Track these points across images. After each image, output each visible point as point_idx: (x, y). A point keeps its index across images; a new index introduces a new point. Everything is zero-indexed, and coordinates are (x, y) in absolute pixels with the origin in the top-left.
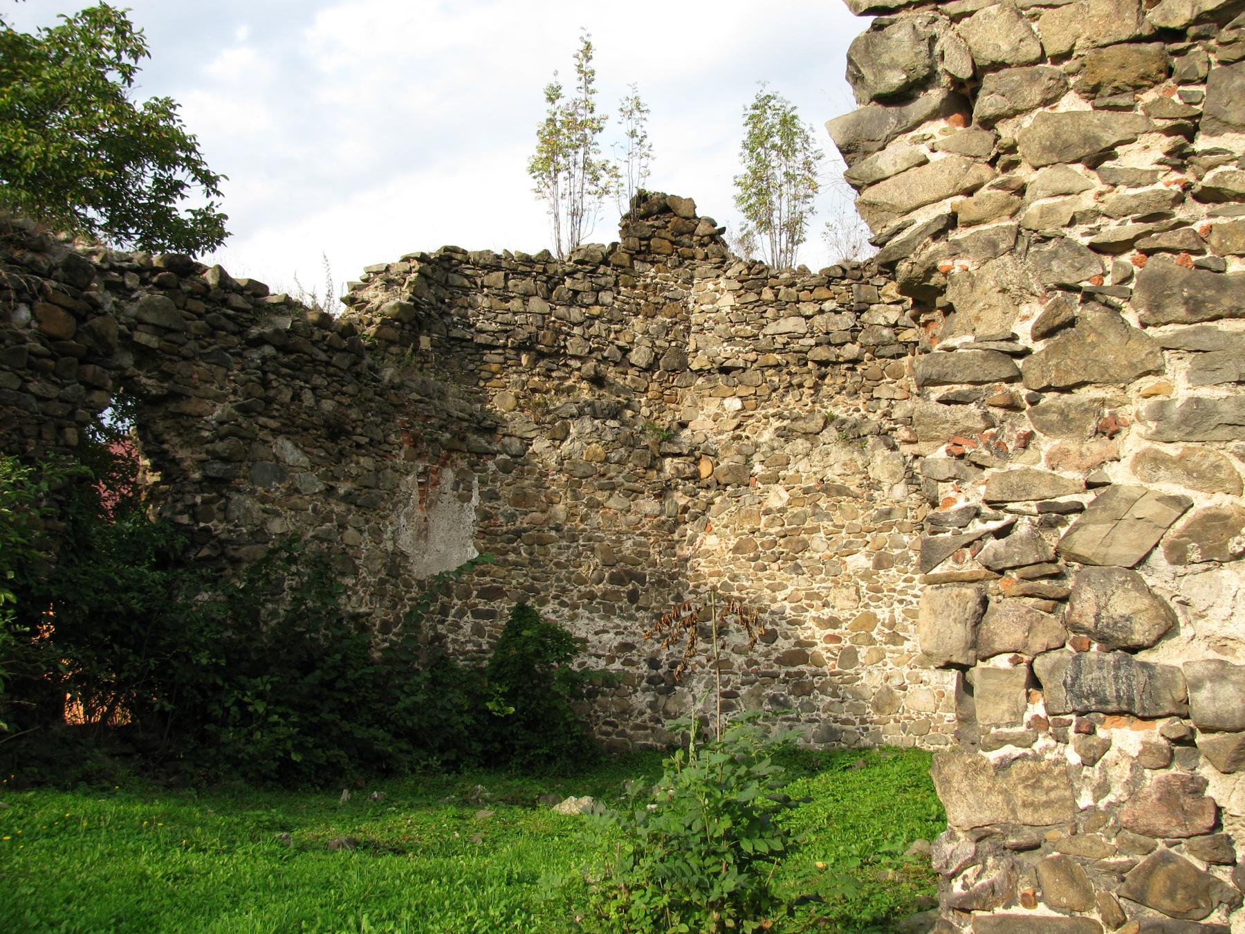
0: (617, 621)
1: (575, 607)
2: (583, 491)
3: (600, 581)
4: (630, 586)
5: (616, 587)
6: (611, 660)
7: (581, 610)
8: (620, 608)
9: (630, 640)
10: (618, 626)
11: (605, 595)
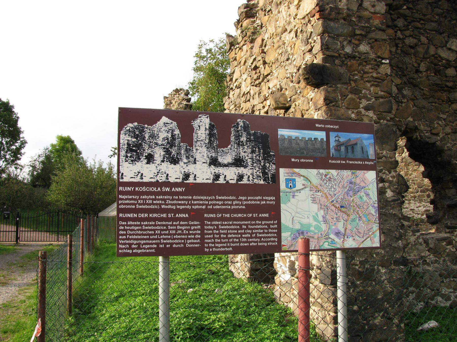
0: (424, 203)
1: (410, 200)
2: (410, 167)
3: (418, 192)
4: (427, 193)
5: (423, 194)
6: (422, 215)
7: (412, 201)
8: (424, 200)
9: (428, 209)
10: (424, 205)
11: (419, 196)
